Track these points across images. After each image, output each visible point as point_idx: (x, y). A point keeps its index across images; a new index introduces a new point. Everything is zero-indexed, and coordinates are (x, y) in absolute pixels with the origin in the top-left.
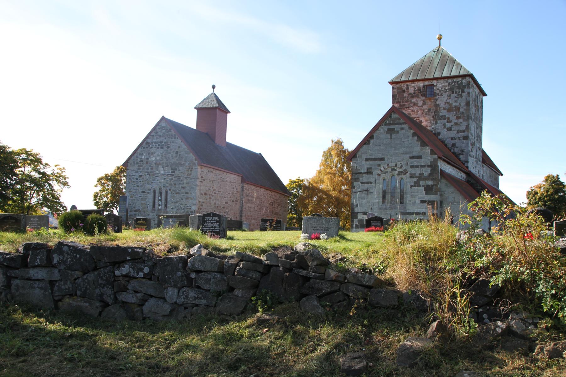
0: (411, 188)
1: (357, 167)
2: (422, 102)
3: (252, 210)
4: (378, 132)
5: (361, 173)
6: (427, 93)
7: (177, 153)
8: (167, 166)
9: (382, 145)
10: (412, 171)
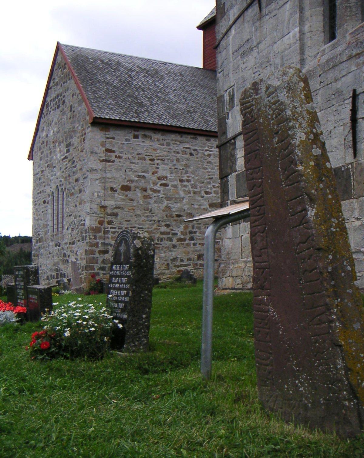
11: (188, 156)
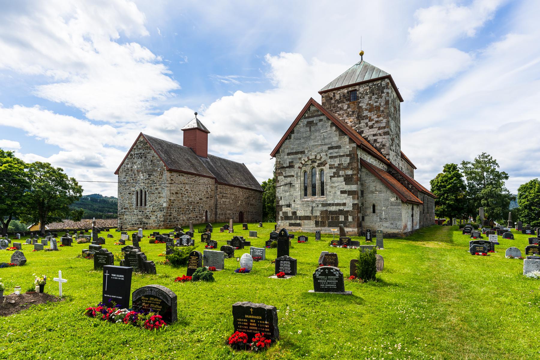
1: (280, 161)
2: (347, 106)
3: (227, 203)
4: (298, 126)
5: (283, 167)
6: (351, 98)
8: (145, 172)
9: (302, 139)
10: (330, 162)
11: (194, 182)
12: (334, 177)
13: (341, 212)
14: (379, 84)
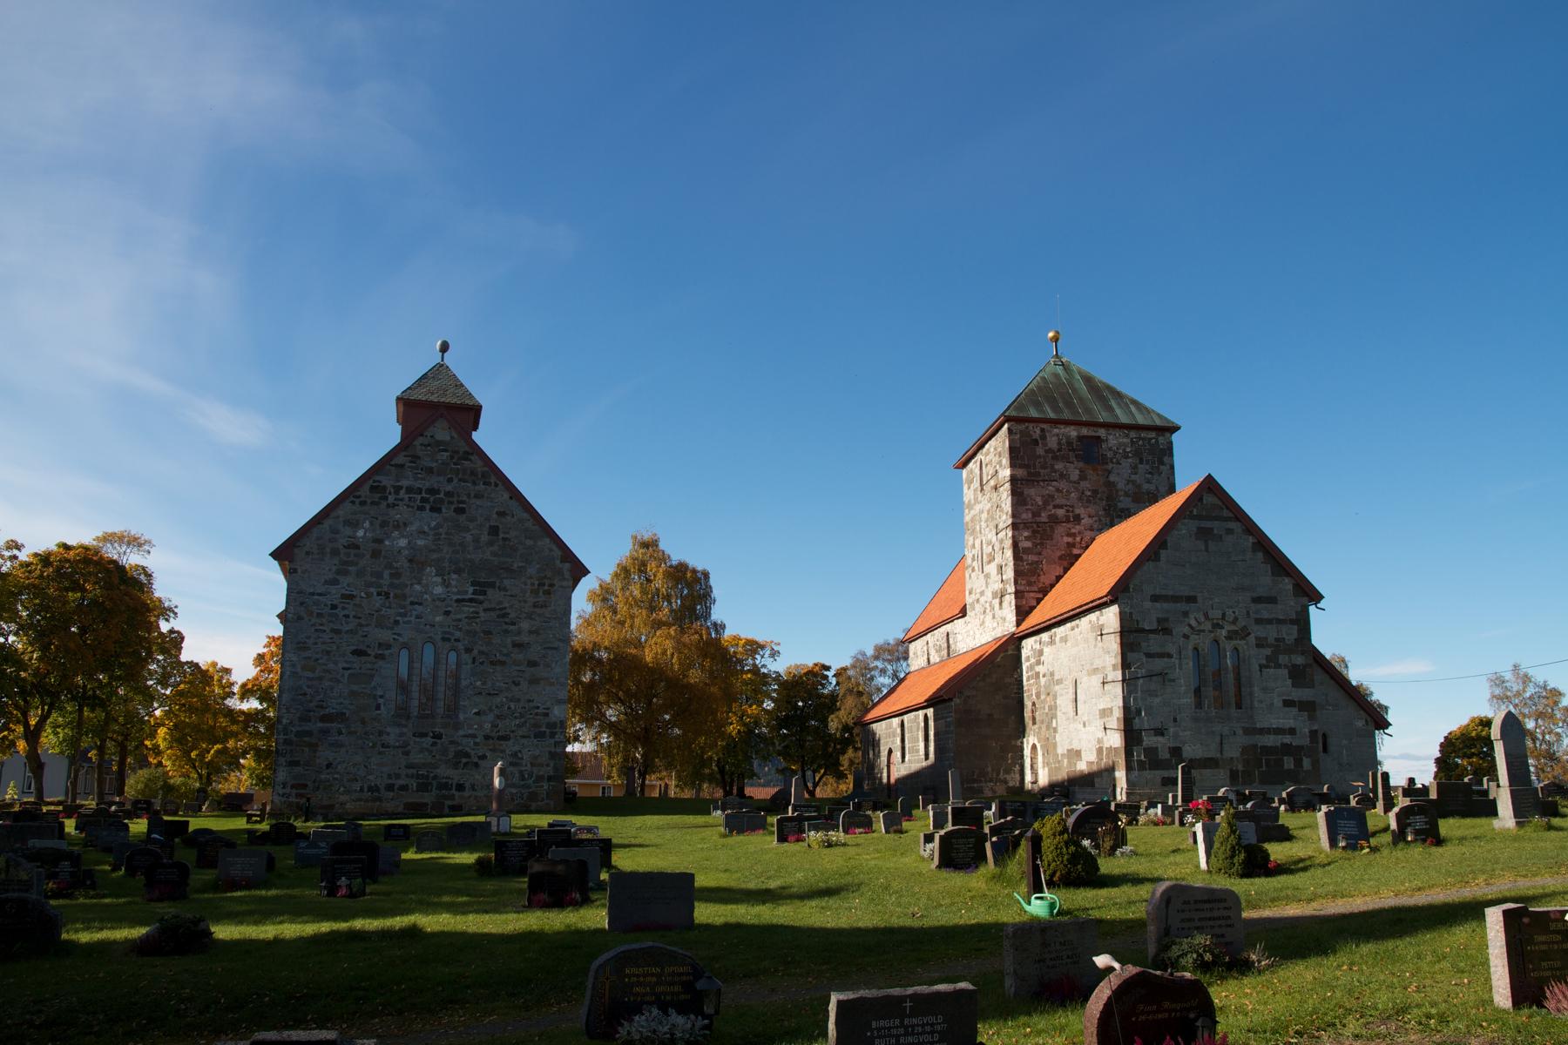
0: (1261, 671)
2: (1077, 472)
5: (1143, 631)
7: (494, 531)
8: (458, 571)
10: (1258, 631)
12: (1267, 667)
13: (1287, 749)
14: (1152, 439)
